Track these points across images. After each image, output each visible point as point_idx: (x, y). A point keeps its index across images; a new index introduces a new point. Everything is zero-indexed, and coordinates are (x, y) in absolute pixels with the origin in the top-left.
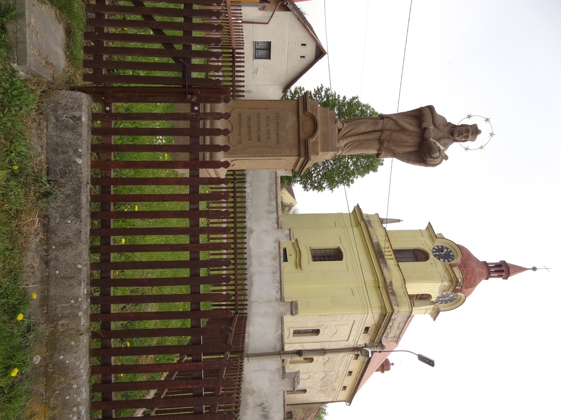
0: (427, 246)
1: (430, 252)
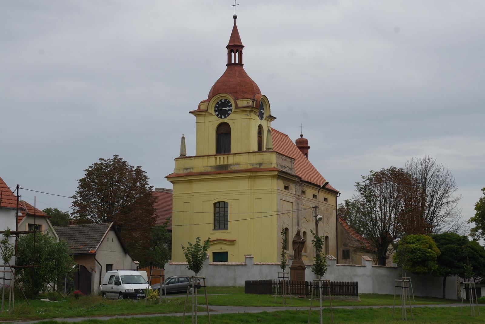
0: (214, 121)
1: (221, 121)
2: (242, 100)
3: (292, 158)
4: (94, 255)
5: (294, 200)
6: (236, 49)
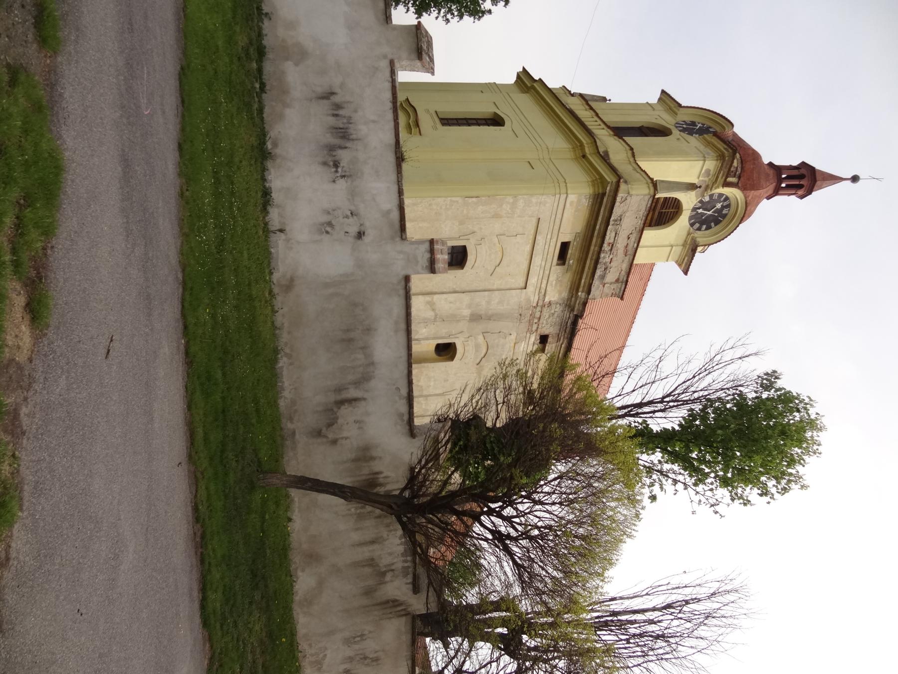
0: (665, 119)
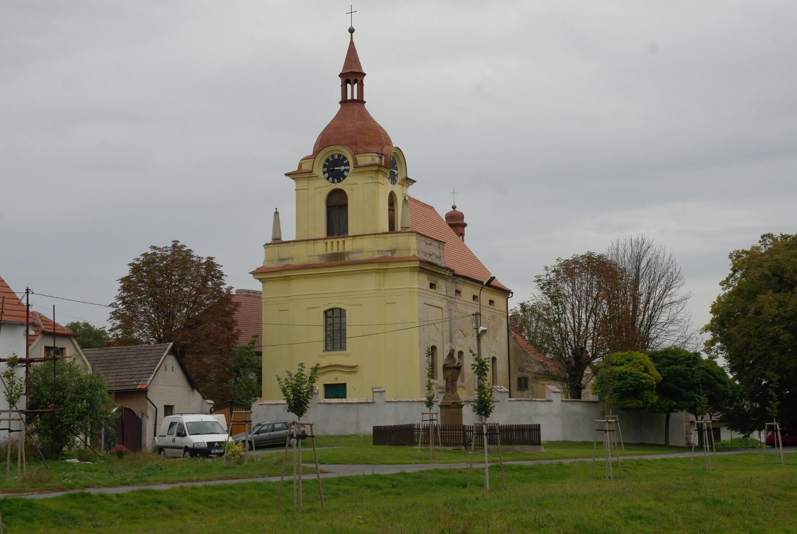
0: (323, 186)
1: (334, 186)
2: (364, 155)
3: (440, 241)
4: (144, 392)
5: (445, 303)
6: (354, 78)
